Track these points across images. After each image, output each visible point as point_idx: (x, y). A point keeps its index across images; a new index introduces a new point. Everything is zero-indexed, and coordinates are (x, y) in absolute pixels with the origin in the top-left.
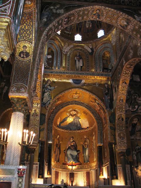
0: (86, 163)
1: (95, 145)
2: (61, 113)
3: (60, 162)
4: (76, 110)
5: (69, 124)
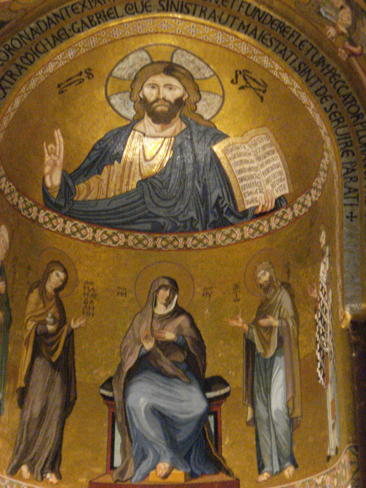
0: (272, 474)
1: (329, 328)
2: (61, 89)
3: (63, 469)
4: (179, 59)
5: (139, 183)
